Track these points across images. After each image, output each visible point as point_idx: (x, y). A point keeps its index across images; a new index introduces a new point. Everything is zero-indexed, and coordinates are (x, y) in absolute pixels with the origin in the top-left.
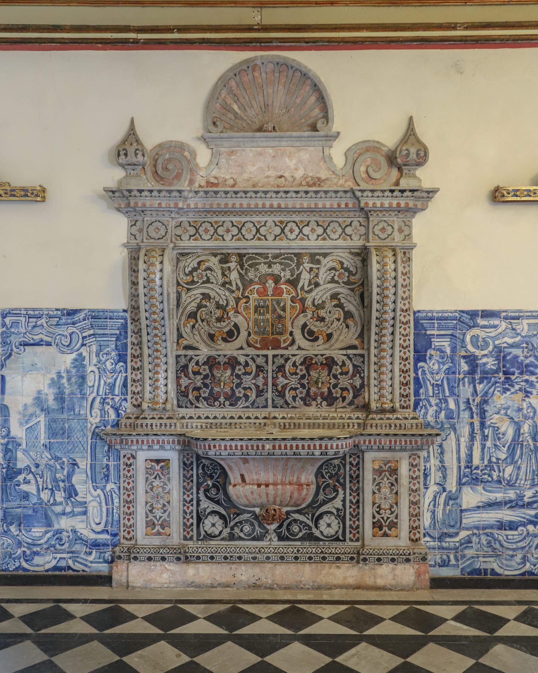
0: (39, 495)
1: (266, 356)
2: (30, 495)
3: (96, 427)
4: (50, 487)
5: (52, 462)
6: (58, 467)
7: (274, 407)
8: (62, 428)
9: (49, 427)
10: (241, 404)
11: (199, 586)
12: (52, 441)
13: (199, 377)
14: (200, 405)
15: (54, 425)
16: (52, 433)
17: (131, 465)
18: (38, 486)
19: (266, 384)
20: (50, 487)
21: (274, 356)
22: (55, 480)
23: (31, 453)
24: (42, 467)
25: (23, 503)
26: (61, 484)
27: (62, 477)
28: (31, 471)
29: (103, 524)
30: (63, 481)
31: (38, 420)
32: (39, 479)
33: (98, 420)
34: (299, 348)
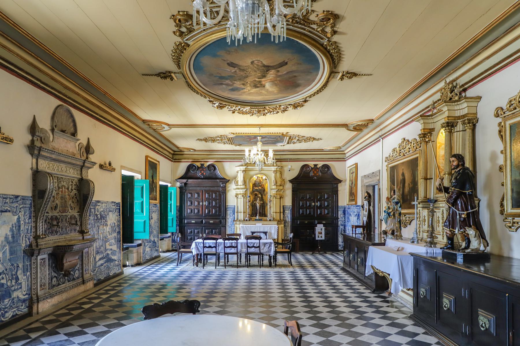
0: (7, 283)
1: (63, 215)
2: (4, 284)
3: (24, 248)
4: (11, 279)
5: (11, 267)
6: (13, 269)
7: (65, 234)
8: (14, 251)
9: (10, 251)
10: (58, 234)
11: (69, 299)
12: (11, 257)
13: (49, 224)
14: (49, 236)
15: (11, 249)
16: (11, 253)
17: (35, 263)
18: (7, 279)
19: (63, 226)
20: (11, 279)
21: (65, 215)
22: (12, 275)
23: (4, 264)
24: (8, 270)
25: (2, 289)
26: (14, 277)
27: (15, 273)
28: (4, 273)
29: (26, 291)
30: (15, 275)
31: (6, 248)
32: (7, 276)
33: (24, 245)
34: (70, 213)
